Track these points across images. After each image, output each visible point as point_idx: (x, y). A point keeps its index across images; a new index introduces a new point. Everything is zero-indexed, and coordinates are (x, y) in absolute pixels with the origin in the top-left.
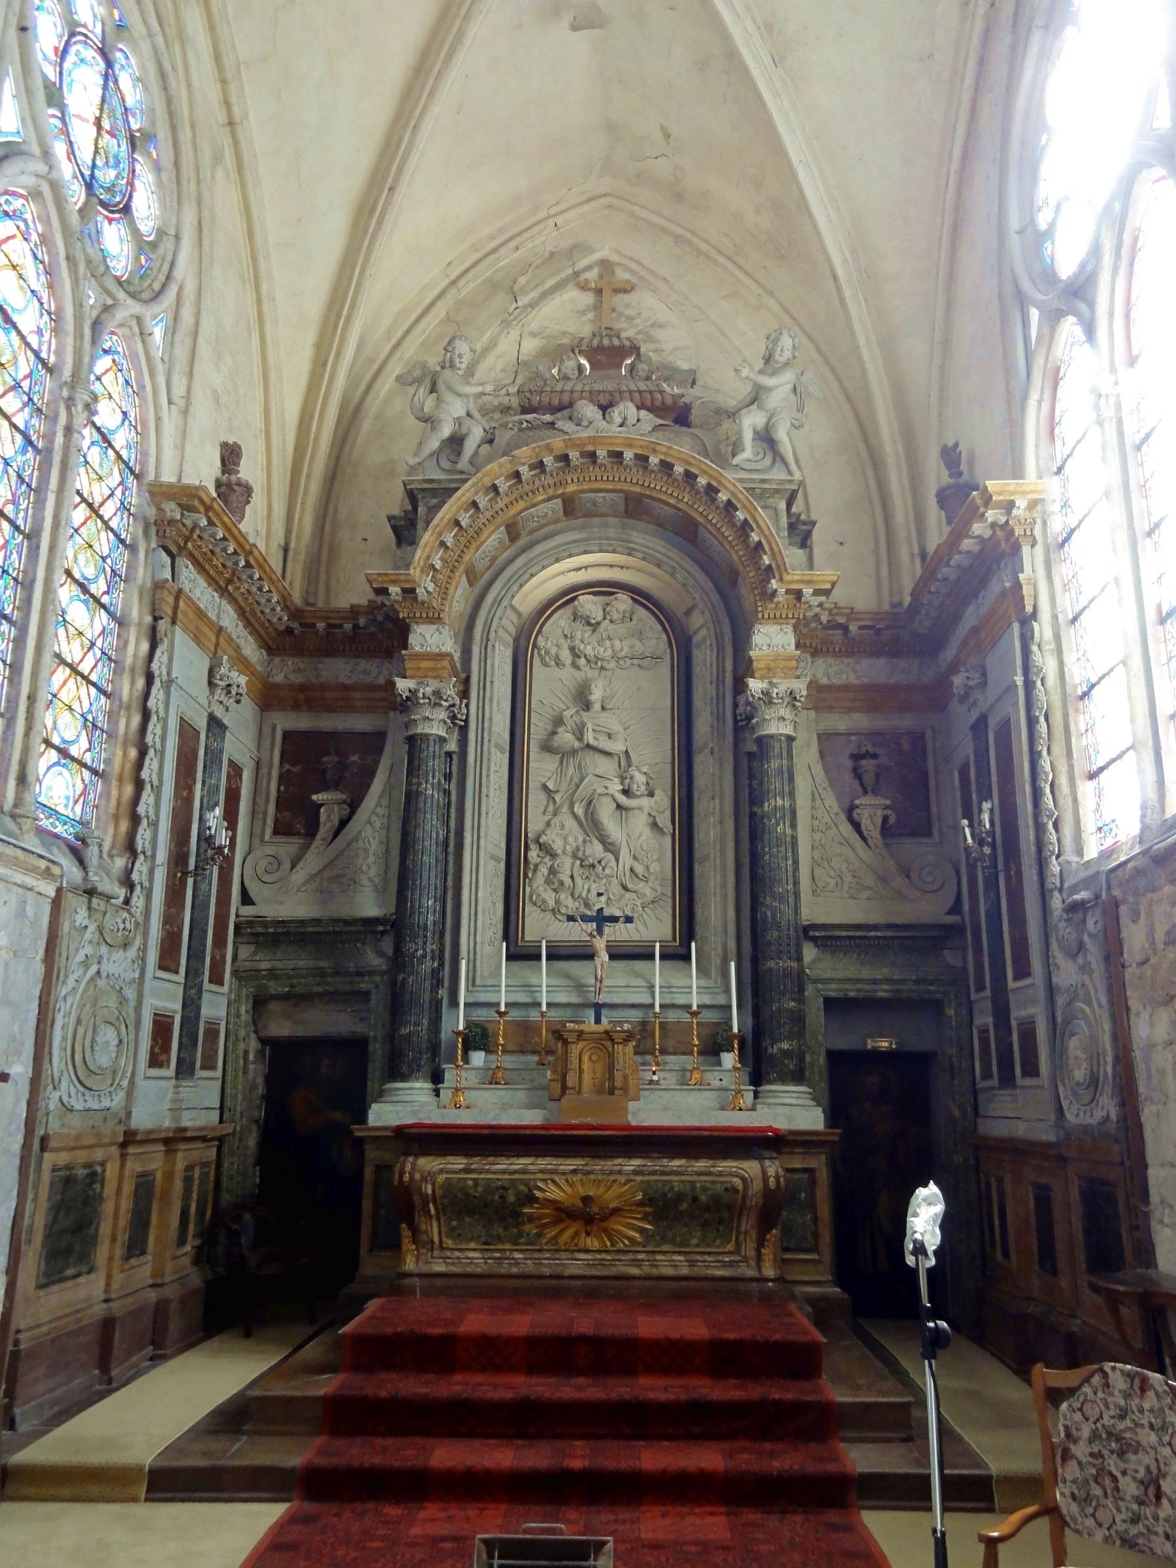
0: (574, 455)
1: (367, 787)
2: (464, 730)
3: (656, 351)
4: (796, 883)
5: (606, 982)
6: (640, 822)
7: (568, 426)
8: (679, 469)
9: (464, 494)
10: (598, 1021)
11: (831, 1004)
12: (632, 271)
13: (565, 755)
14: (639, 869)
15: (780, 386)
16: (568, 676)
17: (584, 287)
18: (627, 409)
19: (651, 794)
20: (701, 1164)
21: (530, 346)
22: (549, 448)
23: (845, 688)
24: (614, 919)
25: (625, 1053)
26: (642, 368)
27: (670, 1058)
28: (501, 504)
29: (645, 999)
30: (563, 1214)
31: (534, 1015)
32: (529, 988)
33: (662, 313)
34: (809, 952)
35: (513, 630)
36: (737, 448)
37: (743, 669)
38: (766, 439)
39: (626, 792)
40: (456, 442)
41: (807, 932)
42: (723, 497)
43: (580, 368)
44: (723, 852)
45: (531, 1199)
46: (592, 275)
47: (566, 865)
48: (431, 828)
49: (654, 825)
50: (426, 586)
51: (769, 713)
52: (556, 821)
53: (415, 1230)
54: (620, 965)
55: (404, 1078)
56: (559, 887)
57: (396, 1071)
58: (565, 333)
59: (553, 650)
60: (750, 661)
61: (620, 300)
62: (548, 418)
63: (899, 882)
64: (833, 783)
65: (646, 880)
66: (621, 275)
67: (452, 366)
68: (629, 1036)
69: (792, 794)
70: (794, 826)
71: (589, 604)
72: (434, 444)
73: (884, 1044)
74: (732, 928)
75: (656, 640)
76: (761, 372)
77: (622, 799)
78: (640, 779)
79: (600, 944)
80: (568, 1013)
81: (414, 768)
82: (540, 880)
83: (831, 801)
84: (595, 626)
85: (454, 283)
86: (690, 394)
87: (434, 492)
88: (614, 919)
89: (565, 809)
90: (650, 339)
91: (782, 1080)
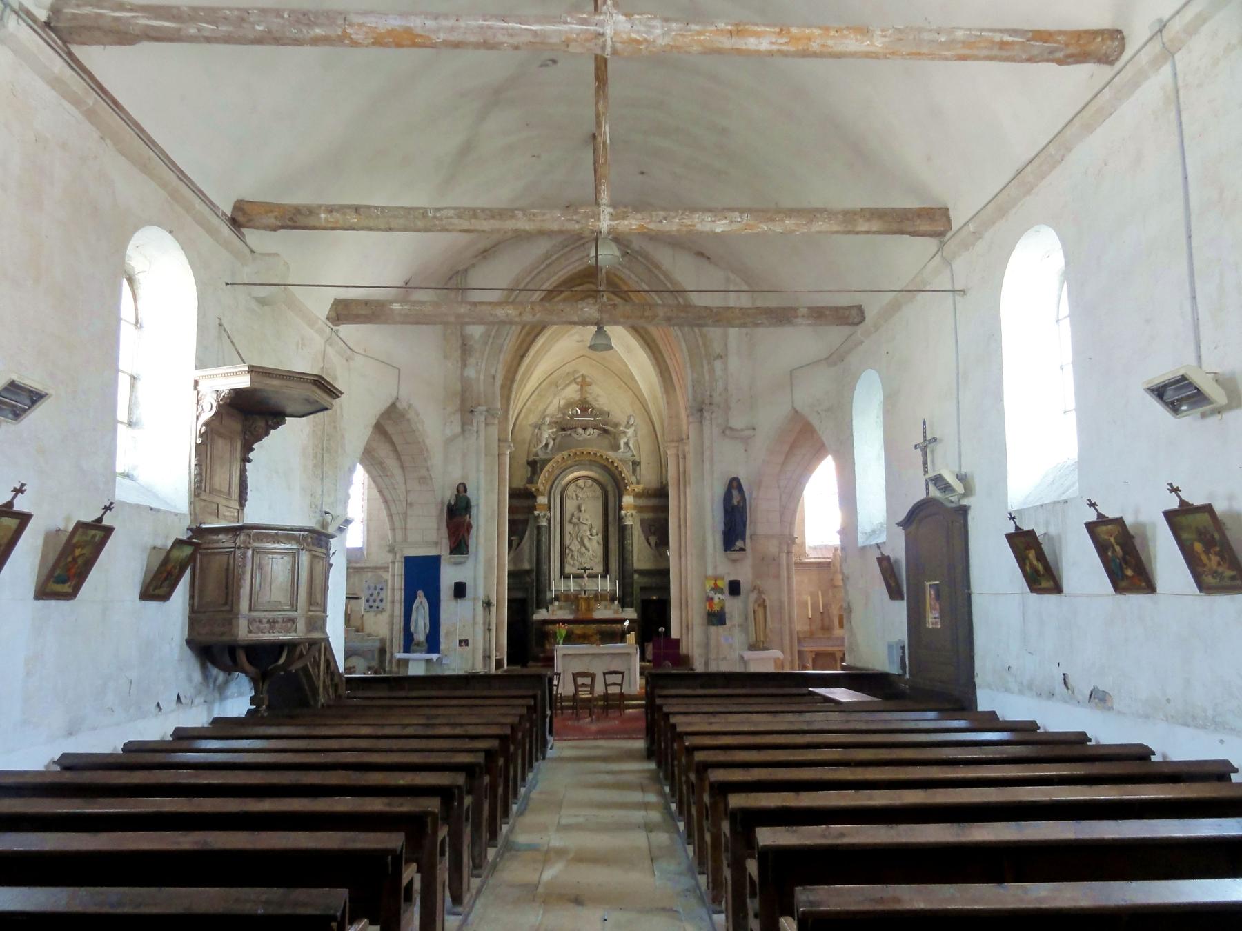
0: (578, 453)
4: (633, 561)
6: (595, 542)
8: (604, 457)
9: (550, 464)
11: (643, 589)
13: (575, 525)
14: (594, 554)
15: (630, 431)
17: (577, 384)
18: (590, 431)
19: (597, 535)
20: (609, 625)
21: (562, 403)
22: (572, 452)
24: (589, 569)
25: (592, 602)
31: (569, 593)
32: (568, 586)
34: (636, 576)
37: (621, 508)
38: (627, 444)
39: (591, 535)
40: (547, 445)
42: (616, 464)
46: (579, 380)
47: (576, 554)
48: (544, 548)
49: (598, 543)
50: (541, 488)
51: (627, 519)
54: (590, 579)
57: (539, 606)
58: (572, 398)
59: (571, 495)
61: (587, 388)
62: (569, 432)
64: (643, 531)
66: (588, 380)
67: (544, 423)
68: (593, 598)
69: (632, 539)
70: (632, 546)
71: (580, 482)
72: (541, 446)
73: (655, 598)
74: (618, 571)
75: (599, 492)
76: (626, 427)
77: (590, 537)
78: (594, 531)
79: (585, 575)
81: (539, 534)
83: (643, 538)
84: (582, 489)
85: (540, 384)
88: (589, 569)
89: (575, 539)
90: (596, 401)
91: (628, 607)
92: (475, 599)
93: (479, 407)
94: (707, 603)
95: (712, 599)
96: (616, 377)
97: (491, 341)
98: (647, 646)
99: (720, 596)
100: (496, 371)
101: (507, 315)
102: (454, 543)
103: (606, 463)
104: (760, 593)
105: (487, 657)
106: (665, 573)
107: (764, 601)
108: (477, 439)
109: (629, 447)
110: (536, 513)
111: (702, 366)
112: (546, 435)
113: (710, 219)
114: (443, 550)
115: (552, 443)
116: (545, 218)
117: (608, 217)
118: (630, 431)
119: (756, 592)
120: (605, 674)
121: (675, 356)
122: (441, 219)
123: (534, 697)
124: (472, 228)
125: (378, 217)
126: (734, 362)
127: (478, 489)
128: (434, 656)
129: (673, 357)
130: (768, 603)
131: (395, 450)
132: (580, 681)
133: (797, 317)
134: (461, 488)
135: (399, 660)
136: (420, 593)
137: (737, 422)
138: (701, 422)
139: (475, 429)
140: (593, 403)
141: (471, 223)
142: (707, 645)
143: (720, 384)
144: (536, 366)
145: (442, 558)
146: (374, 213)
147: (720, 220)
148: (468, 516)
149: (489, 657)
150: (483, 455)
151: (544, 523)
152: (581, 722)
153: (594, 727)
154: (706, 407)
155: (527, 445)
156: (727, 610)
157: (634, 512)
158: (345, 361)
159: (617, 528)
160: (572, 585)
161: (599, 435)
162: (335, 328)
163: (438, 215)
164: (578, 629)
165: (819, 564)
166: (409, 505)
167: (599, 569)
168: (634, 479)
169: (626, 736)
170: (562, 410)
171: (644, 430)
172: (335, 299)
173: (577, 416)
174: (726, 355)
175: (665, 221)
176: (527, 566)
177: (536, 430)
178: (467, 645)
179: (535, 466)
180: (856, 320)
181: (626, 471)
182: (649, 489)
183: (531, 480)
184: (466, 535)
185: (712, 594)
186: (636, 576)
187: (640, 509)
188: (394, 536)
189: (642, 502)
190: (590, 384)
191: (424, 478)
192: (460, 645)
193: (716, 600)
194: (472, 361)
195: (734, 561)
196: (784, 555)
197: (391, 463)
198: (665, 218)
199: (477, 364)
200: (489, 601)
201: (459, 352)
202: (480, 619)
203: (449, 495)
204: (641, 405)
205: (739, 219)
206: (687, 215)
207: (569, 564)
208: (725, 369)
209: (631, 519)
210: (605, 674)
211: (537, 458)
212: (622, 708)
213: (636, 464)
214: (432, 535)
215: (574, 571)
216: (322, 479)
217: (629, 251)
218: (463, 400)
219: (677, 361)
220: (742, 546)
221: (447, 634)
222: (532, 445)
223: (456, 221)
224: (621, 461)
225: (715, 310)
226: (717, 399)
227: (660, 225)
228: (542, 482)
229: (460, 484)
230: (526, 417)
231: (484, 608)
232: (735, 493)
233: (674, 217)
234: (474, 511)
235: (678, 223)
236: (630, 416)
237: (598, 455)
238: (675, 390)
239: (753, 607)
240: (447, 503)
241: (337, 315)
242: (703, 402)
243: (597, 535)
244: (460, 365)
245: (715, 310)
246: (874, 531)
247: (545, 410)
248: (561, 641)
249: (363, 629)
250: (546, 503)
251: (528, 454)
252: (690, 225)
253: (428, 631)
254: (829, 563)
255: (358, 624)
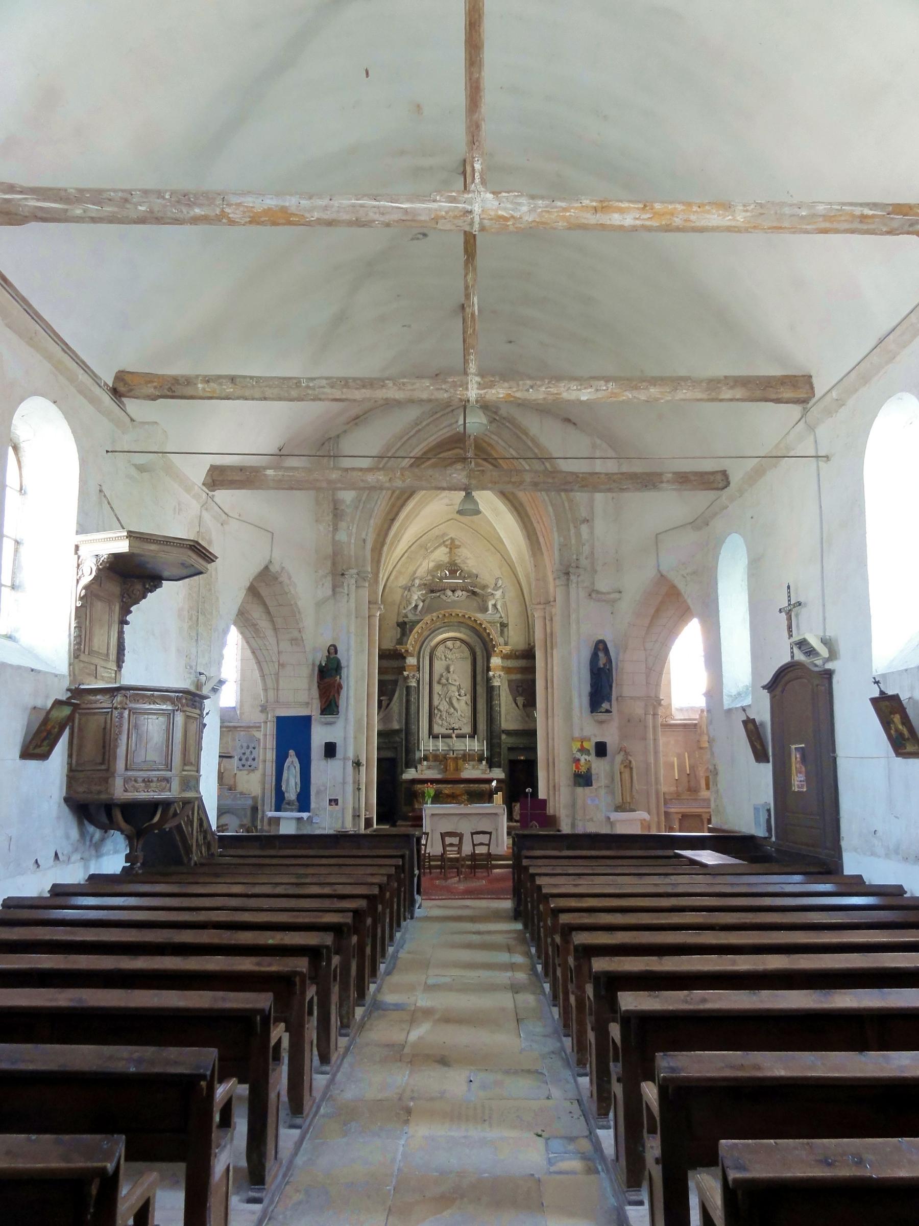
0: (447, 615)
1: (394, 695)
2: (418, 682)
3: (467, 566)
5: (456, 744)
6: (463, 703)
7: (443, 597)
8: (473, 619)
10: (453, 754)
12: (460, 541)
13: (444, 685)
14: (463, 715)
16: (444, 663)
17: (446, 546)
18: (459, 593)
19: (466, 695)
20: (477, 785)
21: (432, 565)
23: (515, 668)
25: (460, 762)
26: (463, 574)
27: (470, 762)
28: (428, 626)
29: (464, 748)
30: (448, 796)
31: (438, 753)
33: (469, 555)
34: (504, 737)
35: (429, 651)
36: (486, 610)
37: (489, 669)
38: (495, 606)
39: (459, 695)
40: (416, 606)
41: (503, 731)
42: (483, 626)
43: (446, 573)
44: (484, 712)
45: (441, 793)
47: (444, 714)
48: (413, 708)
49: (466, 703)
51: (494, 680)
52: (441, 703)
53: (417, 800)
54: (458, 739)
55: (410, 768)
56: (442, 720)
59: (440, 656)
60: (490, 667)
61: (456, 551)
62: (438, 594)
63: (527, 719)
65: (464, 717)
66: (457, 543)
67: (414, 585)
68: (461, 758)
69: (500, 700)
70: (500, 707)
71: (449, 644)
72: (410, 608)
73: (522, 758)
75: (467, 653)
76: (494, 589)
77: (458, 697)
78: (463, 692)
79: (454, 736)
80: (446, 752)
81: (408, 694)
82: (438, 718)
83: (510, 698)
84: (451, 650)
85: (410, 547)
86: (476, 590)
87: (411, 622)
89: (444, 699)
90: (466, 563)
91: (496, 767)
92: (345, 759)
93: (350, 570)
94: (574, 765)
95: (579, 760)
96: (485, 540)
97: (361, 505)
98: (515, 806)
99: (587, 757)
100: (367, 535)
101: (378, 481)
102: (325, 702)
103: (474, 625)
104: (627, 754)
105: (356, 816)
106: (532, 734)
107: (630, 762)
108: (348, 602)
109: (497, 609)
110: (405, 673)
111: (569, 530)
112: (416, 597)
113: (575, 388)
114: (313, 710)
115: (421, 604)
116: (414, 387)
117: (475, 386)
118: (498, 594)
119: (622, 753)
120: (472, 834)
121: (542, 519)
122: (313, 389)
123: (402, 857)
124: (344, 397)
125: (253, 386)
126: (600, 526)
127: (348, 650)
128: (305, 815)
129: (540, 521)
130: (634, 764)
131: (268, 613)
132: (448, 840)
133: (662, 482)
134: (332, 651)
135: (270, 819)
136: (292, 752)
137: (603, 585)
138: (567, 585)
139: (346, 591)
140: (462, 565)
141: (342, 392)
142: (574, 805)
143: (586, 549)
144: (406, 529)
145: (313, 718)
146: (249, 382)
147: (585, 388)
148: (338, 677)
149: (359, 816)
150: (353, 617)
151: (413, 684)
152: (449, 881)
153: (462, 887)
154: (571, 570)
155: (396, 607)
156: (593, 772)
157: (502, 673)
158: (219, 525)
159: (485, 688)
160: (441, 745)
161: (468, 597)
162: (211, 493)
163: (311, 385)
164: (447, 789)
165: (685, 726)
166: (282, 665)
167: (467, 729)
168: (501, 640)
169: (494, 896)
170: (430, 572)
171: (512, 593)
172: (211, 466)
173: (446, 578)
174: (593, 520)
175: (531, 390)
176: (396, 726)
177: (406, 592)
178: (337, 804)
179: (404, 627)
180: (721, 485)
181: (494, 634)
182: (517, 651)
183: (400, 642)
184: (336, 695)
185: (578, 755)
186: (504, 737)
187: (508, 670)
188: (266, 696)
189: (510, 663)
190: (459, 547)
191: (296, 639)
192: (330, 804)
193: (582, 761)
194: (343, 525)
195: (601, 722)
196: (651, 716)
197: (264, 624)
198: (532, 387)
199: (348, 527)
200: (359, 761)
201: (331, 516)
202: (350, 779)
203: (320, 657)
204: (509, 569)
205: (604, 388)
206: (553, 384)
207: (438, 724)
208: (592, 532)
209: (499, 680)
210: (472, 834)
211: (406, 619)
212: (489, 868)
213: (504, 626)
214: (303, 697)
215: (443, 731)
216: (197, 640)
217: (497, 418)
218: (334, 564)
219: (544, 525)
220: (608, 708)
221: (318, 793)
222: (402, 607)
223: (328, 390)
224: (489, 622)
225: (581, 475)
226: (584, 562)
227: (526, 393)
228: (411, 643)
229: (331, 646)
230: (396, 578)
231: (354, 768)
232: (601, 655)
233: (540, 386)
234: (344, 672)
235: (544, 391)
236: (498, 578)
237: (467, 616)
238: (542, 554)
239: (620, 770)
240: (318, 663)
241: (213, 481)
242: (569, 566)
243: (466, 695)
244: (331, 529)
245: (581, 475)
246: (739, 694)
247: (415, 572)
248: (429, 802)
249: (235, 787)
250: (416, 663)
251: (398, 614)
252: (557, 394)
253: (298, 790)
254: (695, 725)
255: (232, 783)
